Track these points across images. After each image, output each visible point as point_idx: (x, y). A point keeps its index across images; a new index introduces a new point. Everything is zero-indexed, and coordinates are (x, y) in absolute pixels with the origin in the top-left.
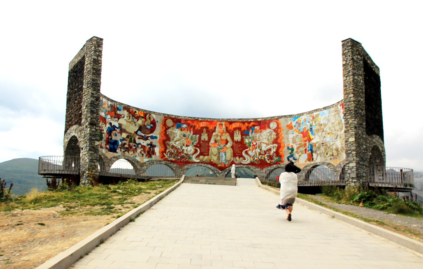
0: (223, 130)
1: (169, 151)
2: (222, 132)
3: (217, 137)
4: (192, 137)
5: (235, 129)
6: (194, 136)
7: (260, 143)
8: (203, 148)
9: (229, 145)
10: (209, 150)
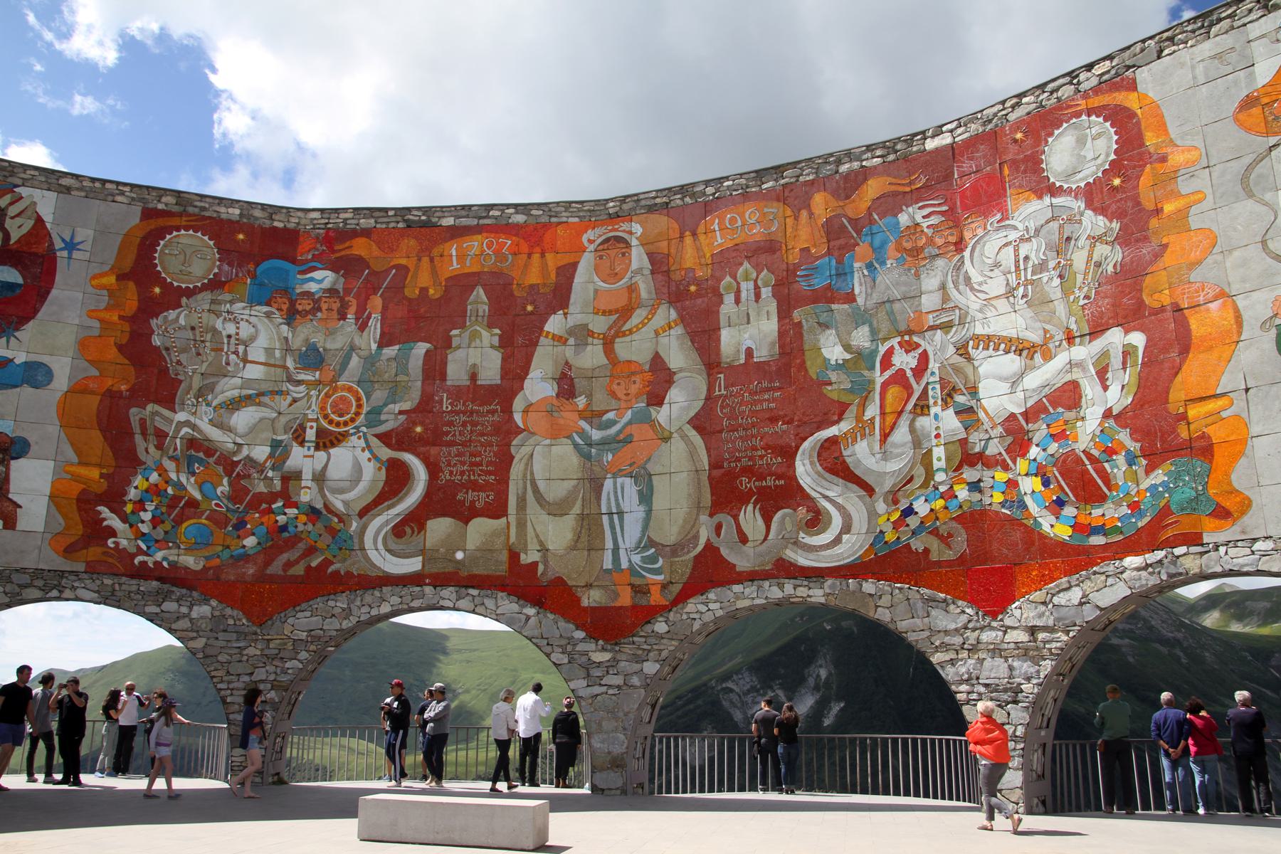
0: (632, 289)
1: (155, 491)
2: (622, 302)
3: (581, 345)
4: (370, 361)
5: (726, 261)
6: (391, 351)
7: (962, 350)
8: (456, 455)
9: (681, 403)
10: (505, 461)
